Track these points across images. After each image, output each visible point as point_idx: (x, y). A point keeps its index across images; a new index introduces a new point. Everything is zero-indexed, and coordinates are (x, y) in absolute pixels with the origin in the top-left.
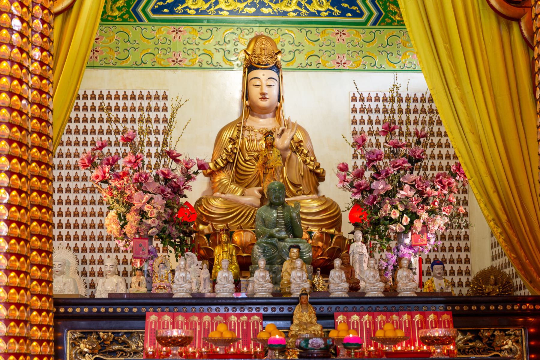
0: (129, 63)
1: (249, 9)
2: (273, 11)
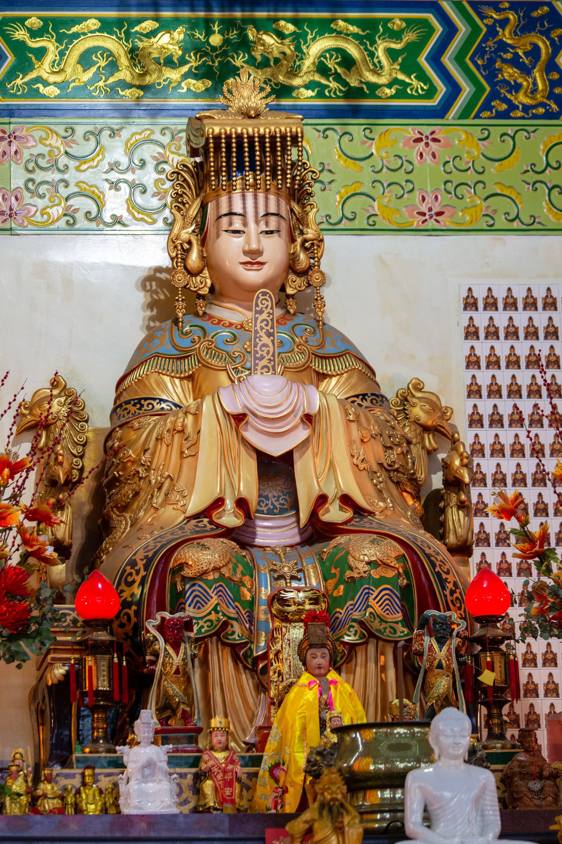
1: (193, 81)
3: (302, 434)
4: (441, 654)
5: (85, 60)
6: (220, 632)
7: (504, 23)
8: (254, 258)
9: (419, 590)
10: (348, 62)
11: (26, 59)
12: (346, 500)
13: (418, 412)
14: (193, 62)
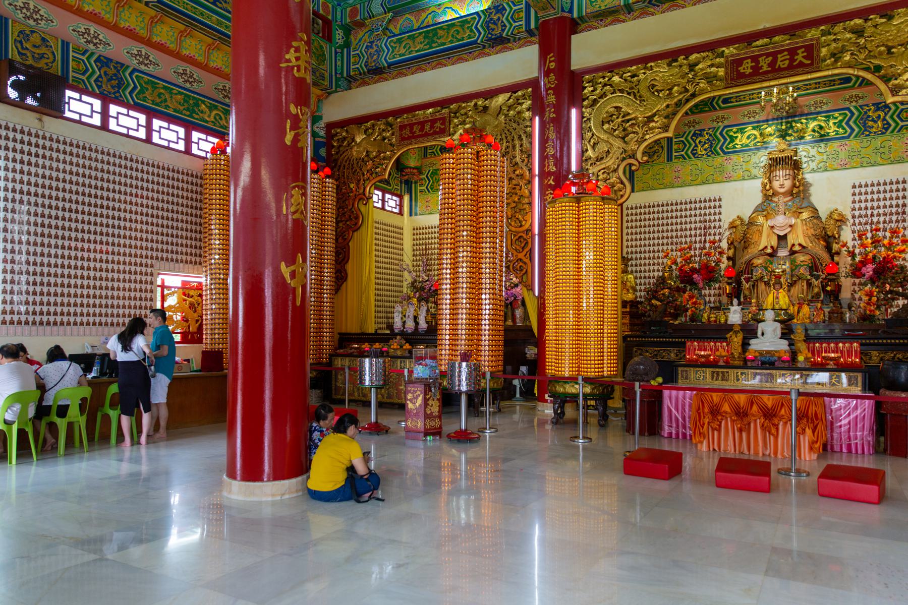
0: (697, 182)
3: (789, 229)
4: (816, 283)
5: (748, 138)
6: (761, 278)
7: (869, 110)
8: (782, 186)
9: (814, 268)
10: (821, 128)
11: (733, 139)
12: (800, 245)
13: (835, 216)
14: (777, 134)
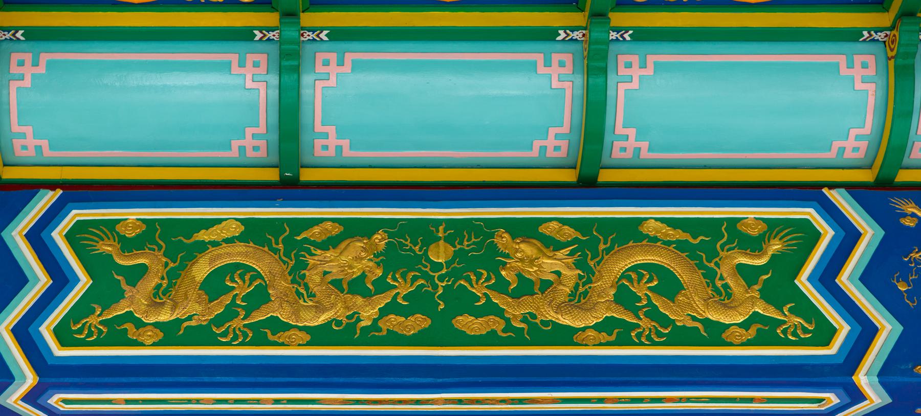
2: (509, 327)
